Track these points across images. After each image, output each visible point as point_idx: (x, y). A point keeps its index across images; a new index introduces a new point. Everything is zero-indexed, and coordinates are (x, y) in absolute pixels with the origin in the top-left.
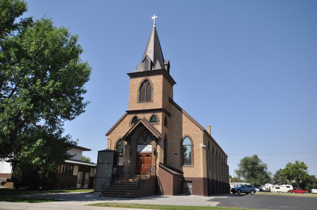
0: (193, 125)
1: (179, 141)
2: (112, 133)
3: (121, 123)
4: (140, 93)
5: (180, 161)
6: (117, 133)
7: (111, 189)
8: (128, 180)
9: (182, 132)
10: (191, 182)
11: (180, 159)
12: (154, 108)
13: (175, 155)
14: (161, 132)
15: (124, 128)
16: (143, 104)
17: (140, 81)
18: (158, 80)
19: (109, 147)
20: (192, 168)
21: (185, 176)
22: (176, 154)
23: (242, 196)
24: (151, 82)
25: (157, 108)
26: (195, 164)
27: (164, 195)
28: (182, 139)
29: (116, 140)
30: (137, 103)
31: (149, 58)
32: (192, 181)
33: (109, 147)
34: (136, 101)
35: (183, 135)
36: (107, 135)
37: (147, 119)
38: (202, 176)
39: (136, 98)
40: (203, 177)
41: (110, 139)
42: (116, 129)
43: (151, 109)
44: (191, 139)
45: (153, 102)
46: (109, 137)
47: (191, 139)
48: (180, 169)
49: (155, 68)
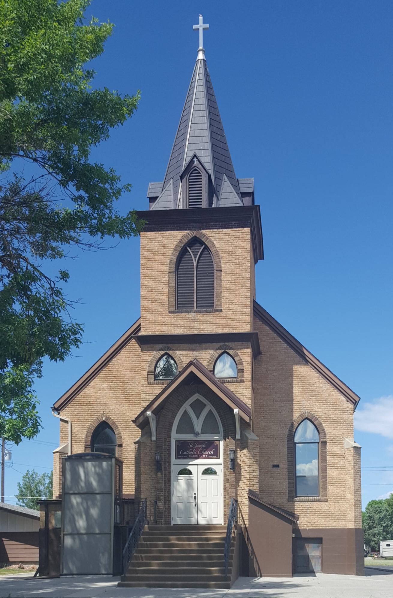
0: (326, 386)
1: (286, 432)
2: (75, 401)
3: (102, 374)
4: (177, 282)
5: (287, 486)
6: (89, 404)
7: (187, 563)
8: (168, 540)
9: (292, 404)
10: (319, 541)
11: (58, 486)
12: (227, 331)
13: (275, 469)
14: (249, 403)
15: (112, 388)
16: (188, 316)
17: (176, 241)
18: (235, 243)
19: (67, 446)
20: (321, 503)
21: (303, 524)
22: (276, 466)
23: (367, 575)
24: (214, 245)
25: (234, 331)
26: (330, 491)
27: (261, 576)
28: (292, 424)
29: (88, 424)
30: (170, 312)
31: (200, 166)
32: (321, 539)
33: (67, 446)
34: (166, 305)
35: (296, 415)
36: (57, 410)
37: (205, 364)
38: (351, 525)
39: (166, 297)
40: (353, 527)
41: (67, 422)
42: (87, 391)
43: (214, 332)
44: (318, 428)
45: (221, 311)
46: (65, 415)
47: (318, 428)
48: (287, 507)
49: (220, 202)
